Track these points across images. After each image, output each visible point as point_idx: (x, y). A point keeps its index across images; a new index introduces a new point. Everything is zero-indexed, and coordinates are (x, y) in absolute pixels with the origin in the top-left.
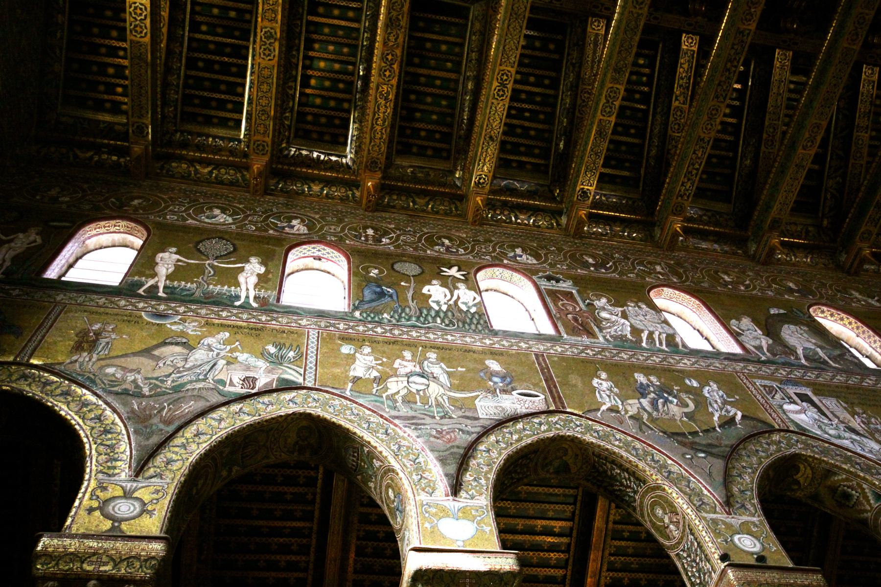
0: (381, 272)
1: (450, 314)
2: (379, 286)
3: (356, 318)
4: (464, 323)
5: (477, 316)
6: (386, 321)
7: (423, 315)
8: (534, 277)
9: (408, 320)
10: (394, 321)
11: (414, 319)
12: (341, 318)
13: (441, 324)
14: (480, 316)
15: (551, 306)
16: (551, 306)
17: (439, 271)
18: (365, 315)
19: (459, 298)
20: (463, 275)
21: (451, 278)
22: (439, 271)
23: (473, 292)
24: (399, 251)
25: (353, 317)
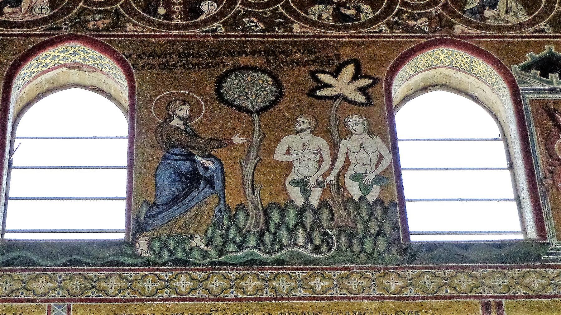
0: (195, 108)
1: (325, 214)
2: (189, 157)
3: (140, 257)
4: (351, 235)
5: (379, 214)
6: (197, 254)
7: (272, 228)
8: (515, 70)
9: (240, 247)
10: (213, 253)
11: (252, 241)
12: (110, 263)
13: (305, 247)
14: (385, 210)
15: (539, 151)
16: (539, 151)
17: (313, 84)
18: (157, 245)
19: (348, 162)
20: (362, 90)
21: (337, 102)
22: (313, 84)
23: (378, 140)
24: (236, 37)
25: (135, 255)
